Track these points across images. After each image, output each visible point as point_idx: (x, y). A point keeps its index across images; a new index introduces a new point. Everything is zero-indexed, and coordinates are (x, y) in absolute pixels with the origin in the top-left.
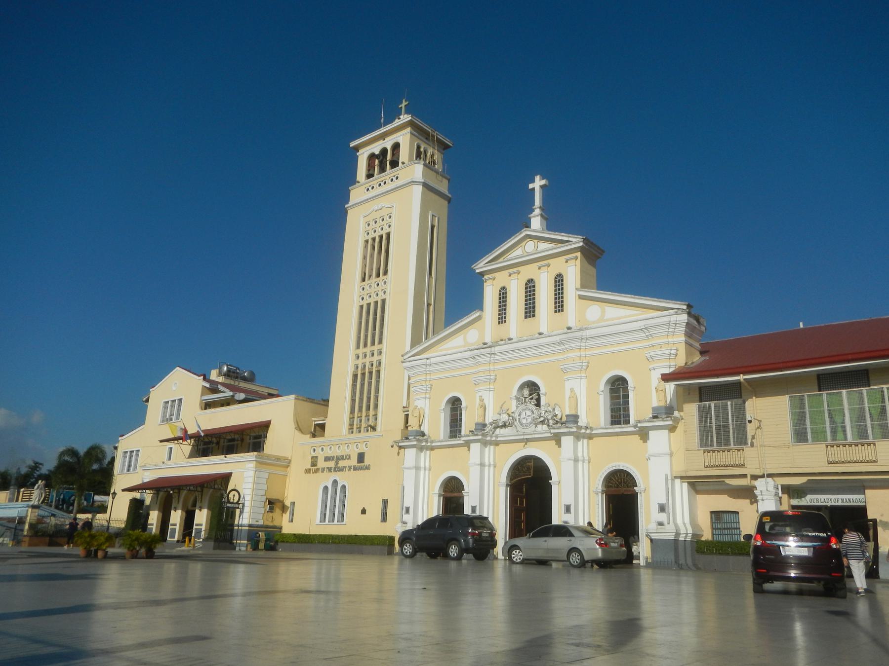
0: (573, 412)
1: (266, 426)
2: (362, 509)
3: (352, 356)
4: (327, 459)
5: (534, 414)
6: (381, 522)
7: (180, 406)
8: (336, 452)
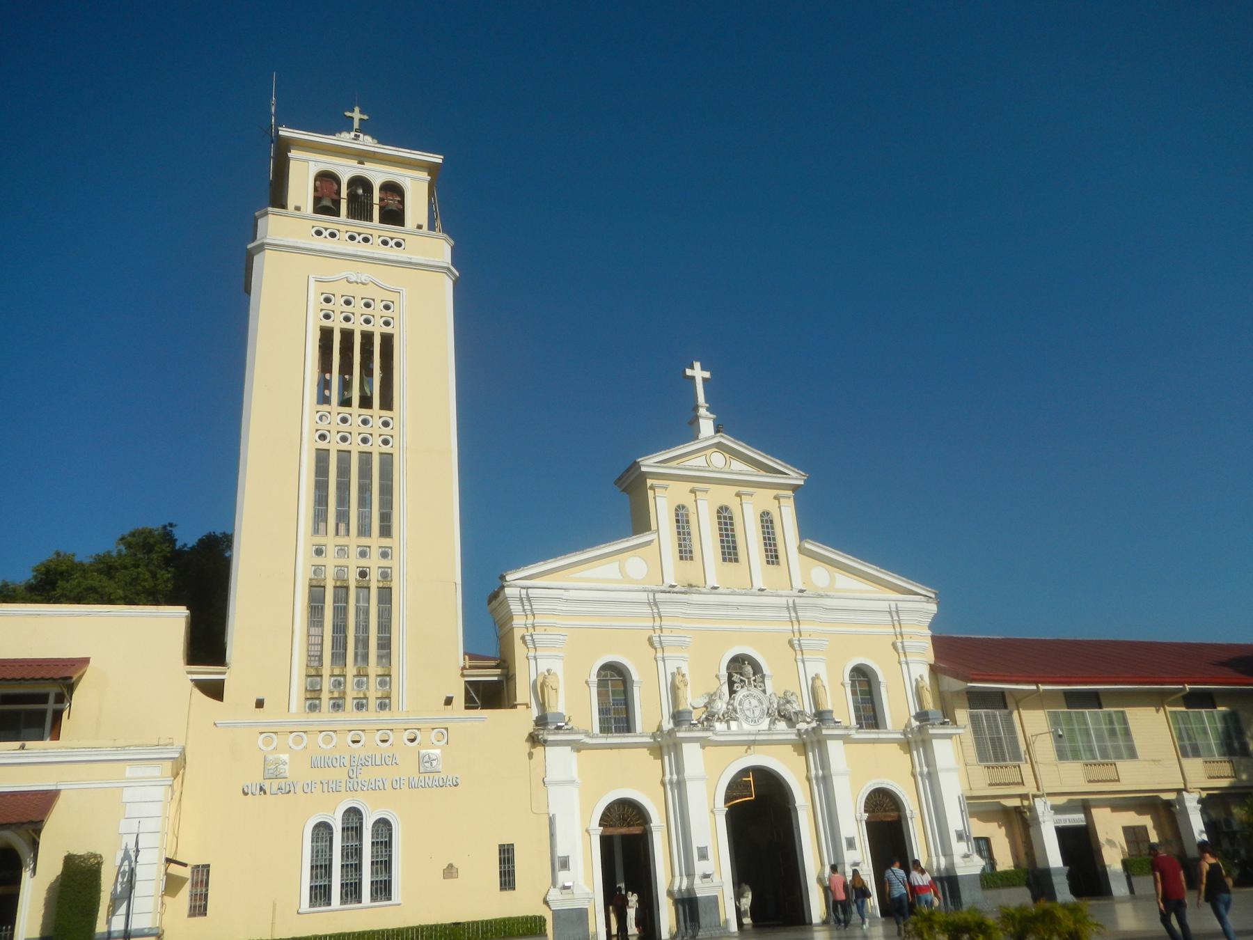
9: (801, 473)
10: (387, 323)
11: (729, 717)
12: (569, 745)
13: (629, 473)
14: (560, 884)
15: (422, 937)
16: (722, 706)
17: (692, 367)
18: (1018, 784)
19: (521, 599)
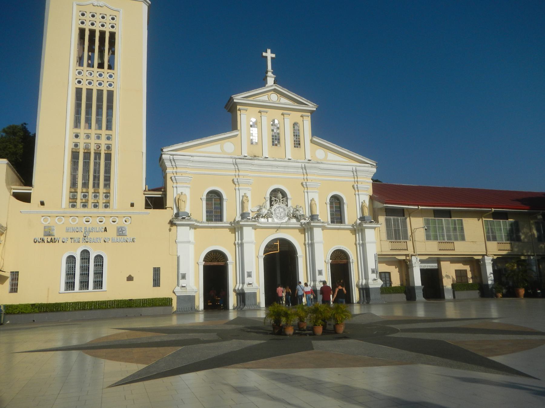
5: (285, 210)
6: (154, 286)
9: (315, 104)
10: (113, 27)
11: (267, 216)
12: (189, 226)
13: (230, 103)
14: (180, 285)
15: (114, 305)
16: (265, 211)
17: (266, 52)
18: (405, 250)
19: (170, 160)
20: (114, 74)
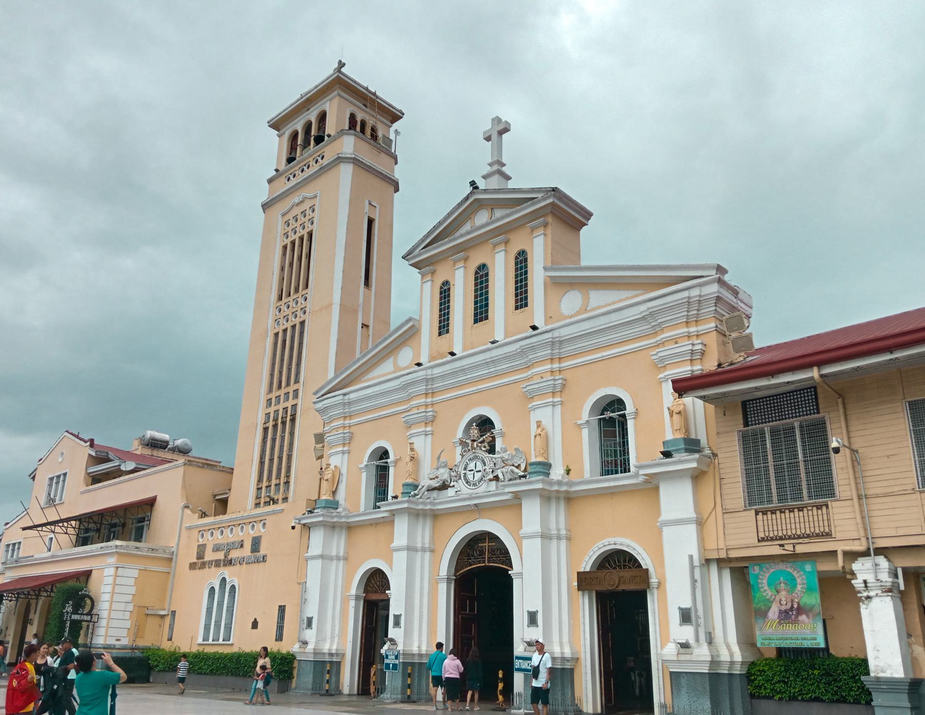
0: (540, 459)
1: (151, 503)
2: (253, 620)
3: (263, 402)
4: (217, 549)
7: (64, 481)
8: (230, 537)
20: (307, 294)
